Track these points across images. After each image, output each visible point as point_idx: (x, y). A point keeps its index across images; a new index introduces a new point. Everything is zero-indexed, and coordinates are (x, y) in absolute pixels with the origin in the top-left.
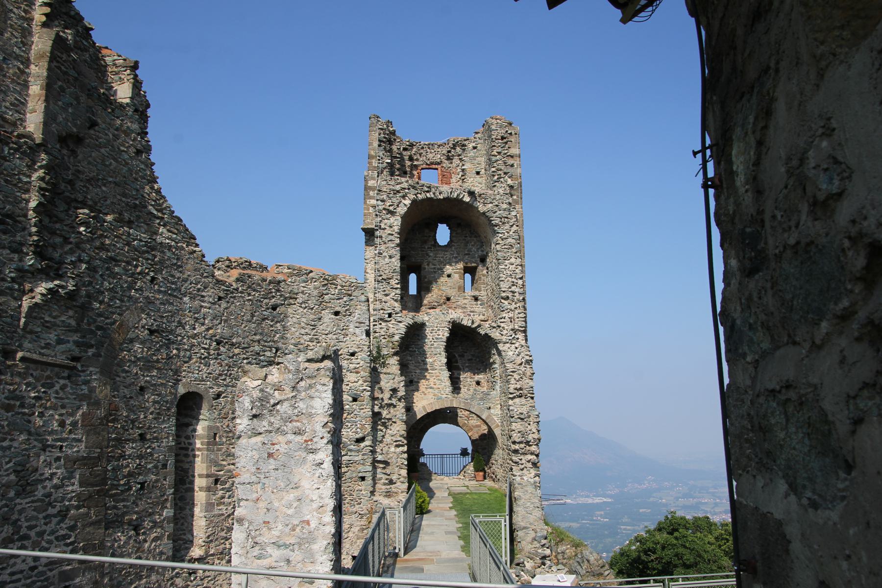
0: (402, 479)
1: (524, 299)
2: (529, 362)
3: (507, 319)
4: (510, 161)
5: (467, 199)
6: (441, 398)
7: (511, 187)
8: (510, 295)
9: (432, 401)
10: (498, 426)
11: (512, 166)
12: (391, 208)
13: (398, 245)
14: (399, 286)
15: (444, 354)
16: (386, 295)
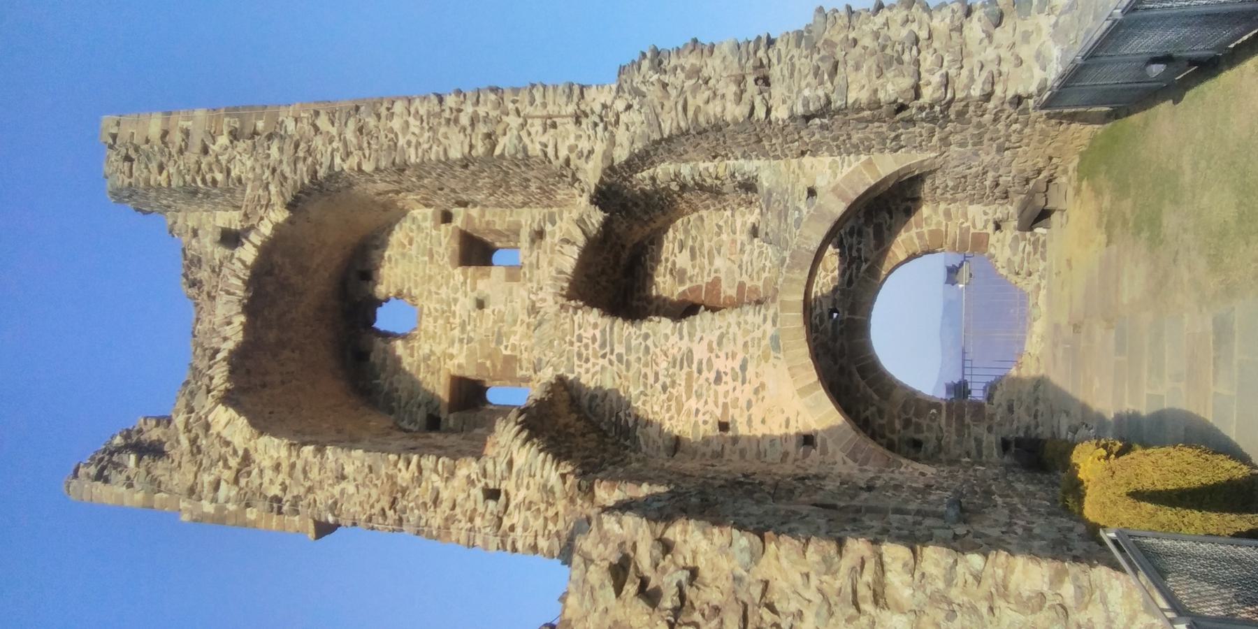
0: (1068, 590)
1: (495, 90)
2: (658, 59)
3: (548, 138)
4: (177, 138)
5: (248, 253)
6: (775, 340)
7: (235, 136)
8: (482, 129)
9: (783, 367)
10: (869, 163)
11: (187, 133)
12: (234, 462)
13: (320, 450)
14: (415, 458)
15: (646, 326)
16: (436, 501)
